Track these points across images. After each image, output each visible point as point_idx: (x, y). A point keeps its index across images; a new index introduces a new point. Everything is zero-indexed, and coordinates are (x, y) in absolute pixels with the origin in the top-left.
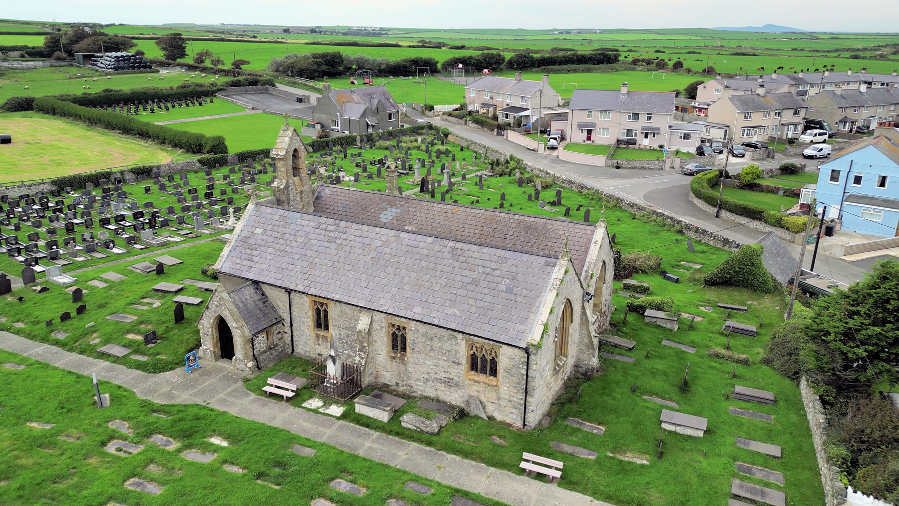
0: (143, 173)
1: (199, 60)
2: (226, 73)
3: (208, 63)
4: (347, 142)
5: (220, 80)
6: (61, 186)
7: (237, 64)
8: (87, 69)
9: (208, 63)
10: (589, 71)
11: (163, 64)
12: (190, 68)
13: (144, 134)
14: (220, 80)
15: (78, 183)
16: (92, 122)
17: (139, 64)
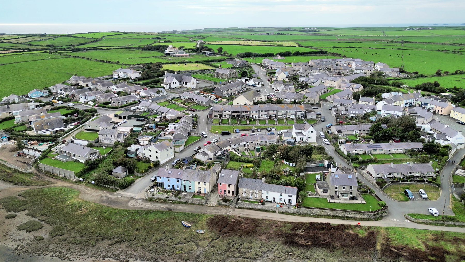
0: (212, 69)
1: (224, 53)
2: (228, 56)
3: (226, 54)
4: (237, 68)
5: (226, 58)
6: (205, 70)
7: (231, 55)
8: (204, 55)
9: (226, 54)
10: (314, 56)
11: (218, 54)
12: (222, 55)
13: (212, 66)
14: (226, 58)
15: (206, 70)
16: (206, 64)
17: (213, 54)
